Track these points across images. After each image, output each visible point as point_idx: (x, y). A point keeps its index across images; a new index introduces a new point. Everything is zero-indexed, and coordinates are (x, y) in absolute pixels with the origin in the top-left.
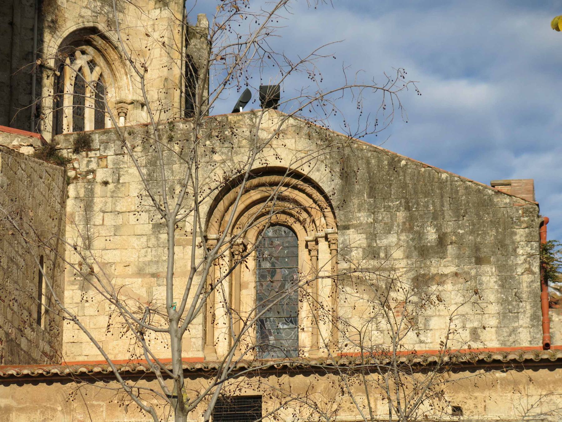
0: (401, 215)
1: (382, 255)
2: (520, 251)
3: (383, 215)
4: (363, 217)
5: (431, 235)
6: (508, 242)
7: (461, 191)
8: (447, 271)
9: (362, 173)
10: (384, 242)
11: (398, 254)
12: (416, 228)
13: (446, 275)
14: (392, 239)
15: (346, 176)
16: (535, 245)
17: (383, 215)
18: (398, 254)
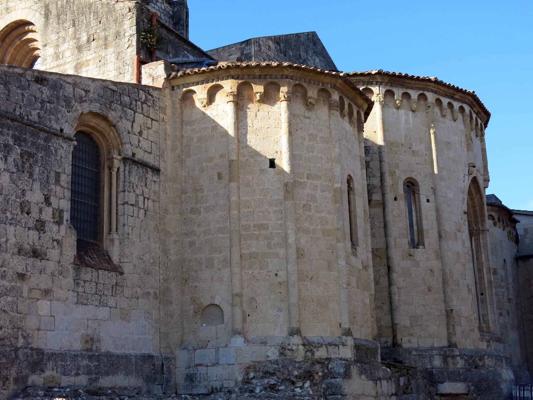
0: (71, 30)
1: (61, 57)
2: (127, 34)
3: (62, 34)
4: (54, 37)
5: (84, 38)
6: (121, 30)
7: (100, 6)
8: (89, 57)
9: (54, 12)
10: (61, 49)
11: (68, 54)
12: (77, 36)
13: (90, 60)
14: (66, 45)
15: (47, 17)
16: (135, 28)
17: (62, 34)
18: (68, 54)
